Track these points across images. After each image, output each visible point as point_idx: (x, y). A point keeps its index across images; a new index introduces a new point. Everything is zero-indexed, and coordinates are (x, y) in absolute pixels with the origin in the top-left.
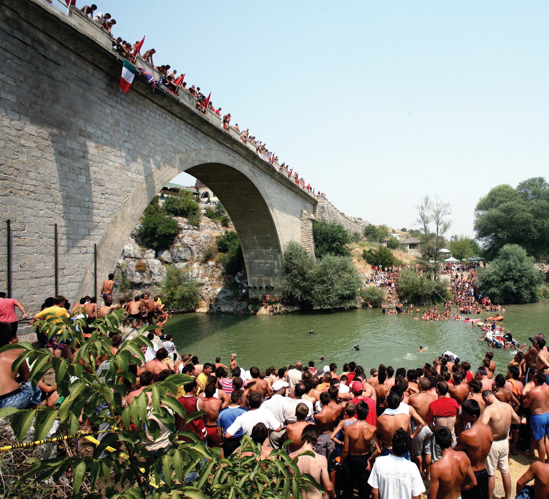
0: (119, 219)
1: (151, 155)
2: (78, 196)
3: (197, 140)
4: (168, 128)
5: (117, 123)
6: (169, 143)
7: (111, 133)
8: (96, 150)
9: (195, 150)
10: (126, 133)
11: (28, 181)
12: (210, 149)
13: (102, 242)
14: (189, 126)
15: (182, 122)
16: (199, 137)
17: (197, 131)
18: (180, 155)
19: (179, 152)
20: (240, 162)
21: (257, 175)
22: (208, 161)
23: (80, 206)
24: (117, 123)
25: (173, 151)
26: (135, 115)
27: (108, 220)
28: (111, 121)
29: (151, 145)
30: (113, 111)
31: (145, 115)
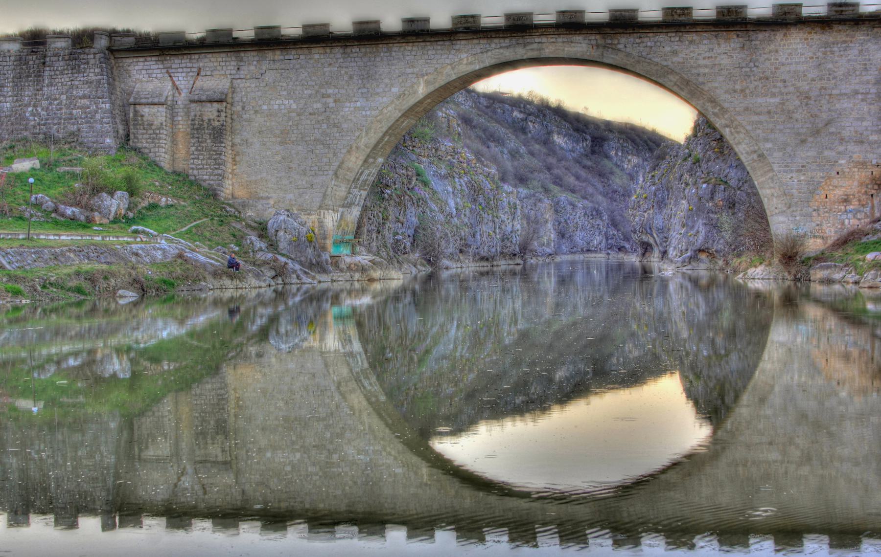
0: (354, 148)
1: (386, 90)
2: (322, 138)
3: (453, 52)
4: (407, 58)
5: (351, 78)
6: (409, 71)
7: (346, 87)
8: (334, 104)
9: (451, 64)
10: (360, 82)
11: (293, 135)
12: (482, 53)
13: (339, 167)
14: (439, 43)
15: (428, 44)
16: (457, 47)
17: (454, 42)
18: (426, 77)
19: (423, 76)
20: (560, 44)
21: (621, 46)
22: (477, 68)
23: (323, 144)
24: (351, 78)
25: (415, 76)
26: (368, 64)
27: (344, 151)
28: (346, 78)
29: (387, 81)
30: (347, 70)
31: (378, 59)
